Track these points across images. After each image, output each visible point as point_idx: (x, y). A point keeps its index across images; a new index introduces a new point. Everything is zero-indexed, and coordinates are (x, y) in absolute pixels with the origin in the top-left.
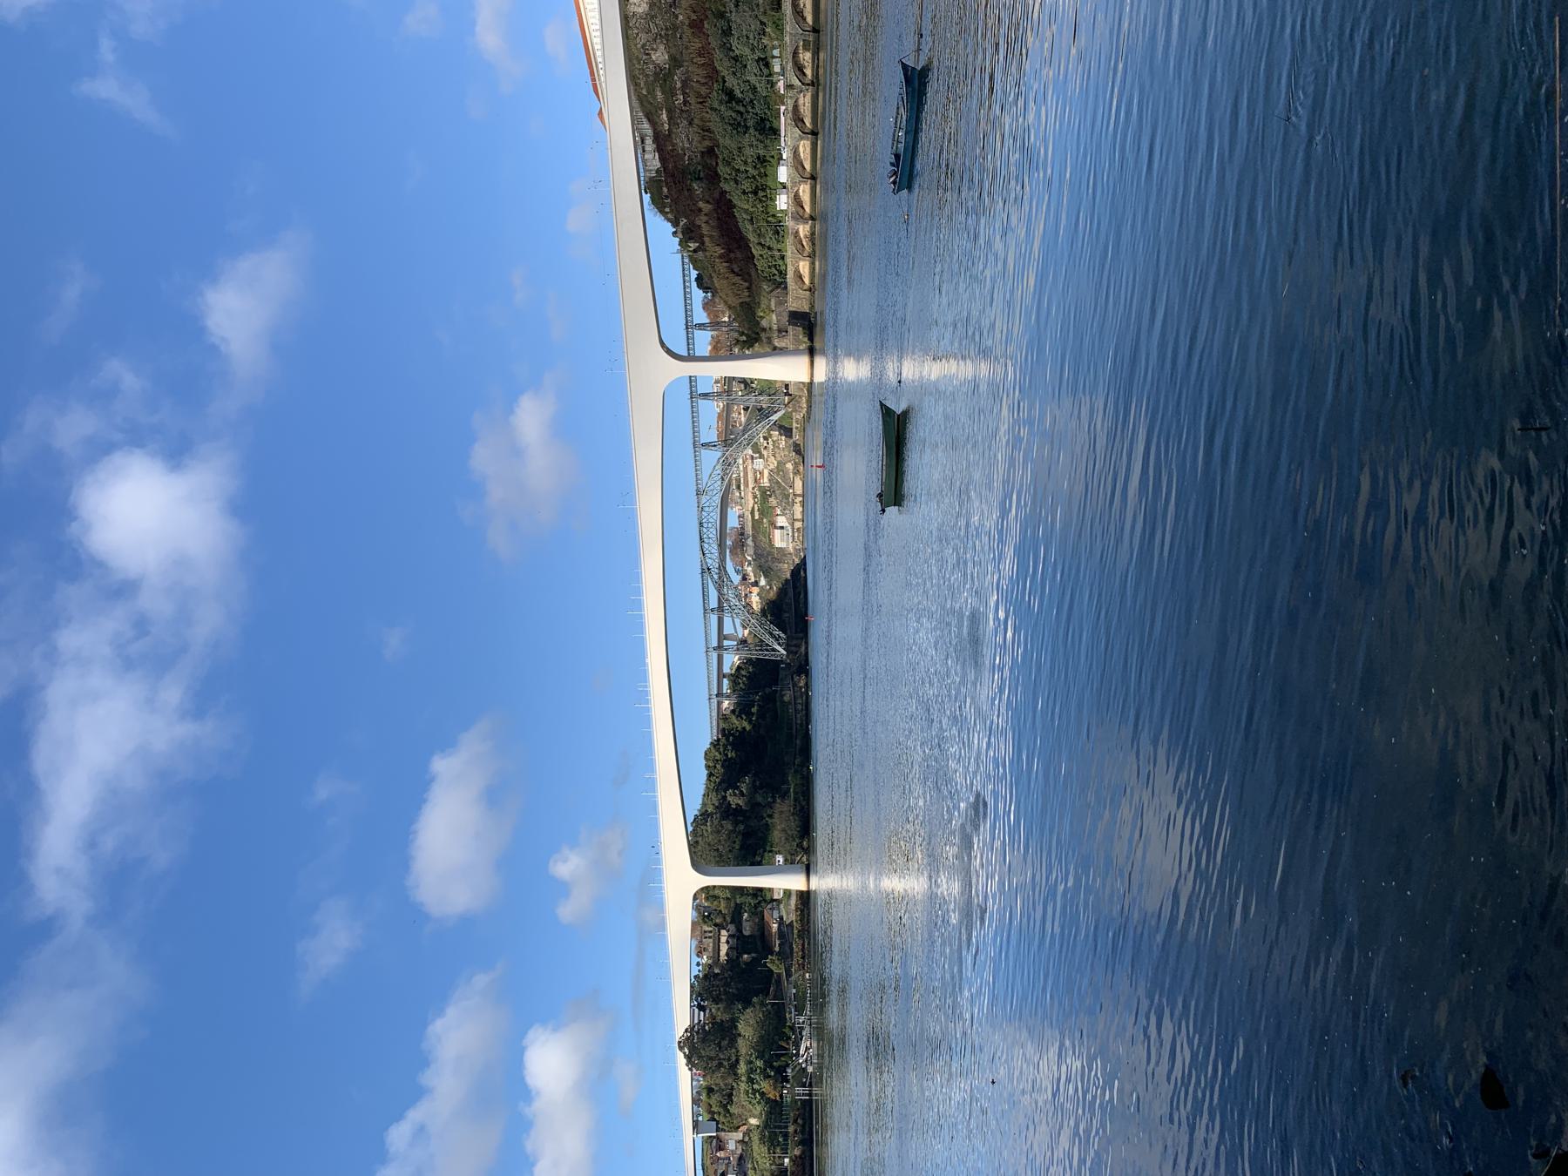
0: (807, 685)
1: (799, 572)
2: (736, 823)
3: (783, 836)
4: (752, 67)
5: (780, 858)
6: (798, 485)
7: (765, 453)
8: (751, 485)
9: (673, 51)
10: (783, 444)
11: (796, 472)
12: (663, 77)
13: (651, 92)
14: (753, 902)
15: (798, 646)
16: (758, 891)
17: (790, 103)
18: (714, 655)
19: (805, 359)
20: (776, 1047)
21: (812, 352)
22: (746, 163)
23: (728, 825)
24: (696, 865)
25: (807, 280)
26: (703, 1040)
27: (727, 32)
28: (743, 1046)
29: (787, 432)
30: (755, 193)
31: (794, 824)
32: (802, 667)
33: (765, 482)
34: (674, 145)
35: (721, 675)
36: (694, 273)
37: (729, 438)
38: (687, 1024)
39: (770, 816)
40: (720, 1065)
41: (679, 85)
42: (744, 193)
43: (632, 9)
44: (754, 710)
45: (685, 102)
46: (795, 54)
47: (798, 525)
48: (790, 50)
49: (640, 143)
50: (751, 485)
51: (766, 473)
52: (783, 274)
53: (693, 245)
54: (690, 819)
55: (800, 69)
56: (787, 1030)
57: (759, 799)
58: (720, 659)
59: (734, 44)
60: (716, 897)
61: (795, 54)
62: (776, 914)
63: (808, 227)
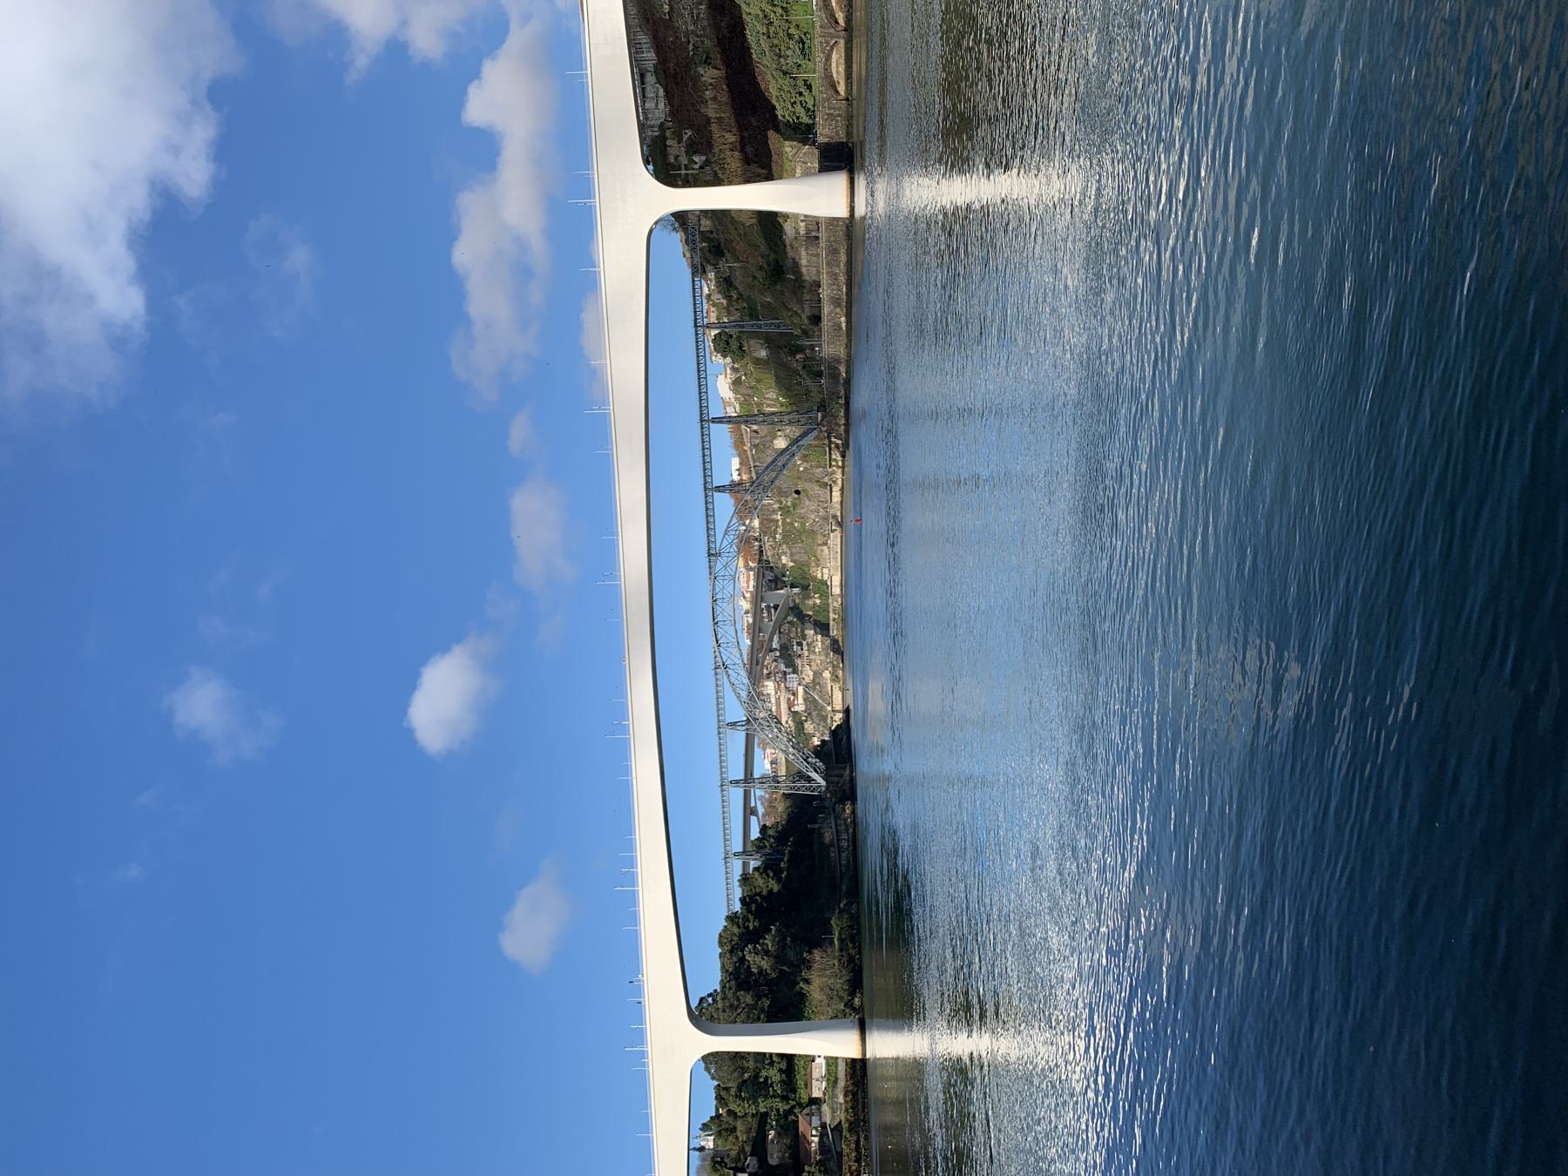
2: (758, 997)
6: (838, 696)
7: (798, 662)
10: (819, 647)
11: (835, 678)
14: (783, 1107)
16: (789, 1058)
29: (823, 628)
31: (840, 984)
33: (800, 707)
34: (676, 31)
39: (807, 981)
49: (639, 77)
51: (801, 689)
54: (694, 1004)
62: (816, 1121)
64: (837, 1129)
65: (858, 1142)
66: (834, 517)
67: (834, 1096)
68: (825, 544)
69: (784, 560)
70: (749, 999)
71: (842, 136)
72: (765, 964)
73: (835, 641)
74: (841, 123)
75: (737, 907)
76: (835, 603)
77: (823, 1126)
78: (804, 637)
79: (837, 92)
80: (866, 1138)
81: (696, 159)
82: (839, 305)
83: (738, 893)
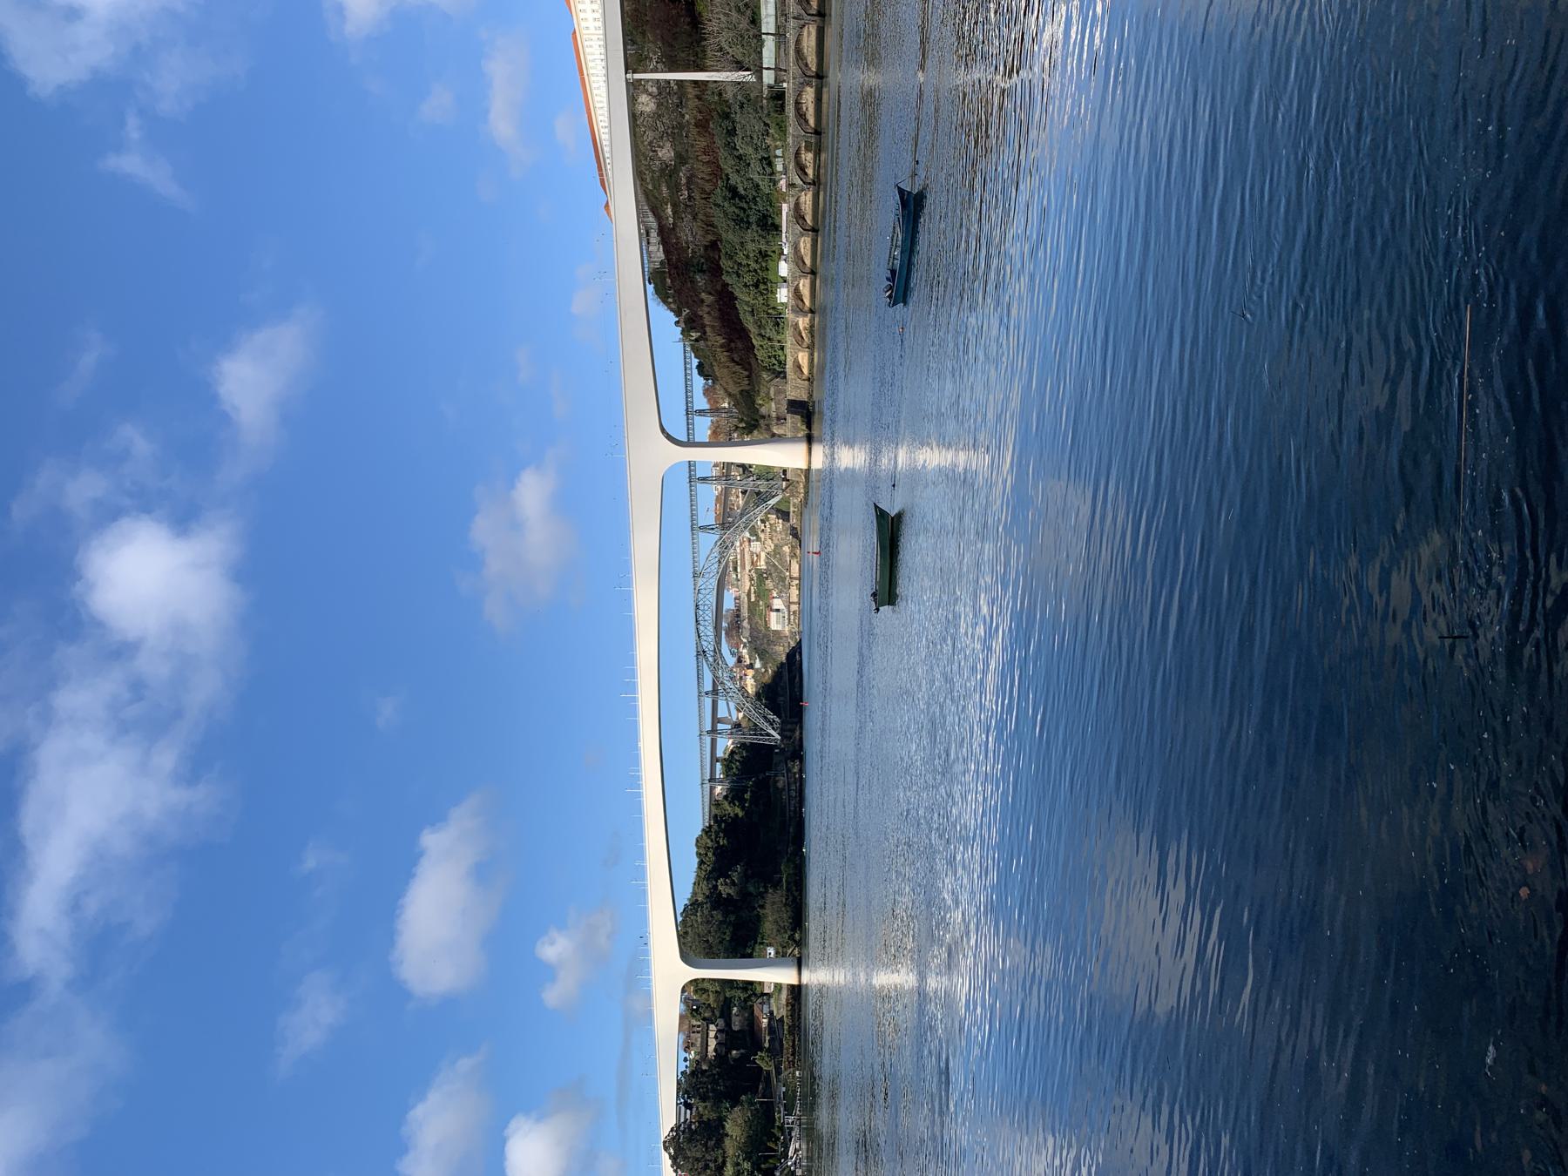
0: (801, 771)
1: (795, 655)
2: (726, 914)
3: (775, 927)
4: (755, 166)
5: (771, 951)
8: (748, 567)
9: (679, 148)
11: (793, 555)
12: (668, 173)
13: (657, 187)
14: (743, 996)
15: (793, 731)
16: (748, 985)
17: (792, 200)
18: (708, 739)
19: (803, 447)
20: (764, 1143)
21: (810, 440)
22: (747, 257)
23: (718, 915)
24: (685, 957)
25: (806, 371)
26: (690, 1140)
27: (732, 132)
28: (730, 1147)
29: (784, 515)
30: (756, 286)
31: (786, 915)
32: (795, 752)
33: (762, 565)
35: (714, 760)
36: (695, 362)
37: (726, 522)
38: (673, 1122)
39: (762, 907)
40: (706, 1167)
41: (684, 181)
42: (746, 285)
43: (640, 108)
44: (747, 796)
45: (690, 197)
46: (797, 154)
47: (794, 607)
48: (792, 151)
49: (645, 235)
50: (748, 567)
51: (763, 555)
52: (782, 364)
53: (695, 335)
54: (680, 909)
55: (801, 168)
56: (775, 1131)
57: (751, 889)
58: (714, 742)
59: (738, 142)
60: (705, 991)
61: (797, 154)
63: (807, 320)
70: (720, 917)
71: (805, 398)
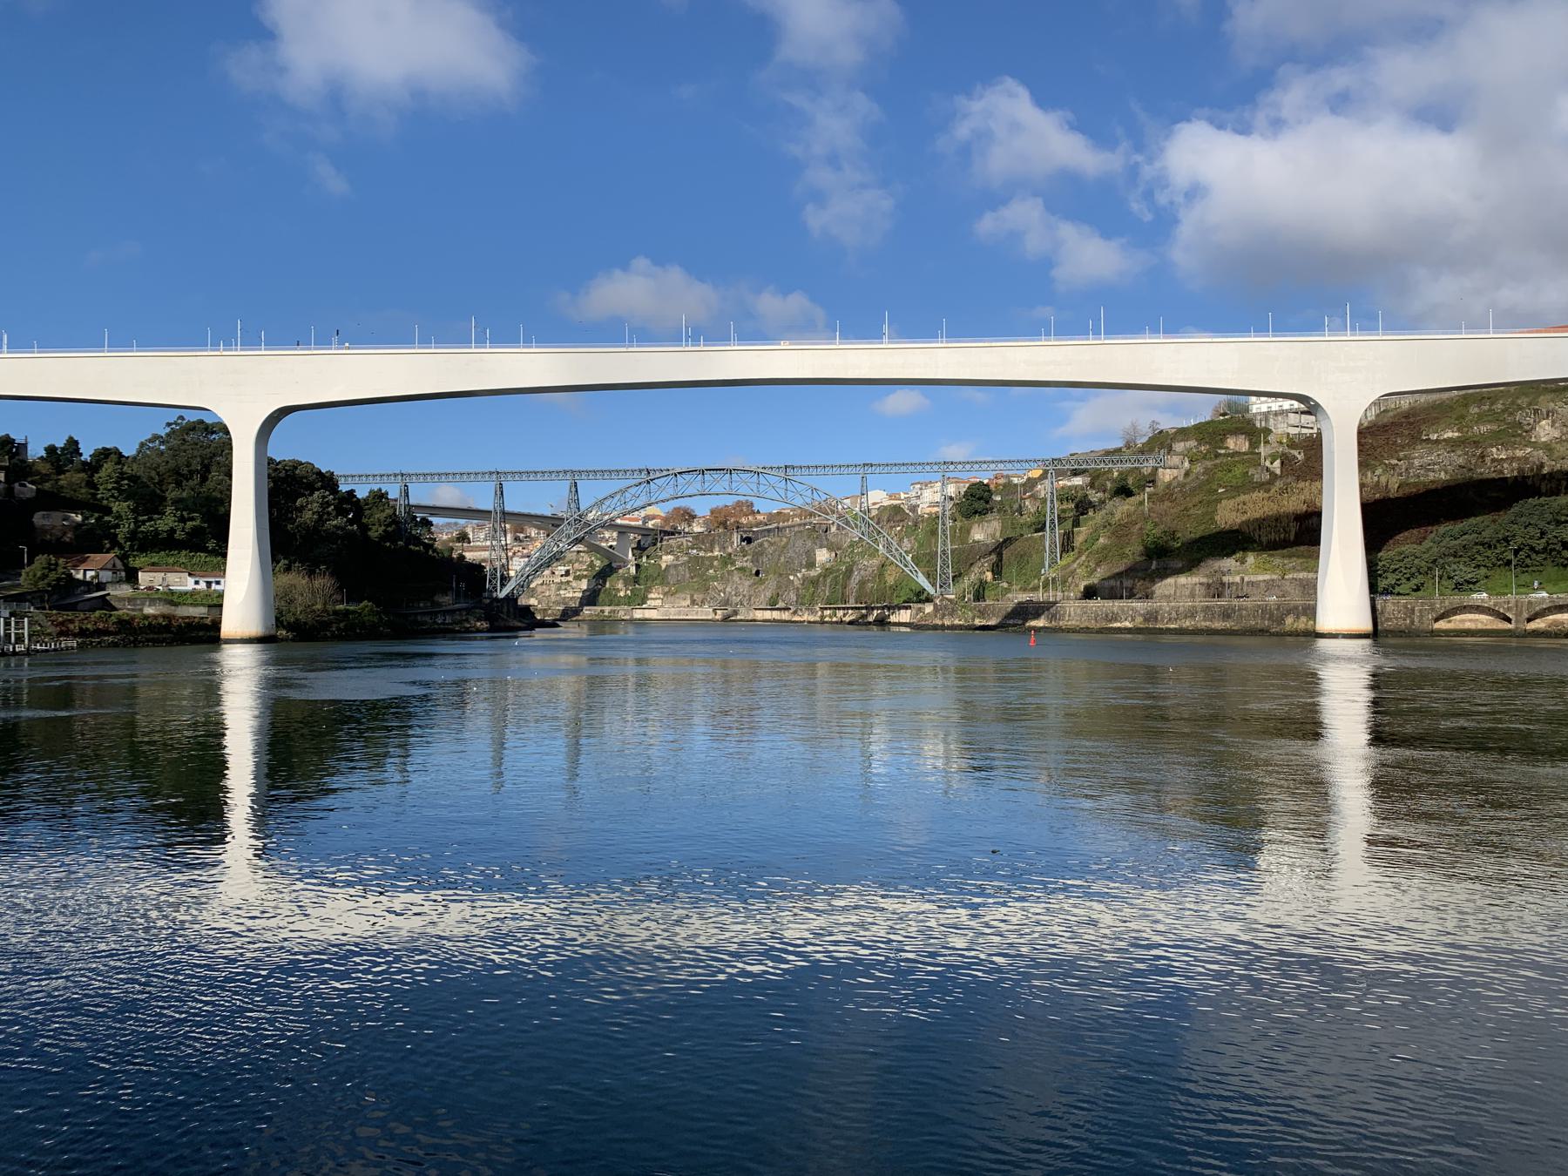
13: (1480, 419)
14: (122, 532)
29: (591, 598)
41: (1519, 453)
62: (106, 576)
64: (104, 603)
65: (106, 632)
66: (736, 613)
67: (153, 602)
68: (693, 602)
69: (667, 559)
72: (308, 516)
73: (576, 612)
74: (1403, 623)
75: (343, 488)
76: (622, 612)
77: (101, 586)
78: (578, 578)
79: (1437, 620)
80: (115, 645)
81: (1277, 463)
82: (1146, 620)
83: (362, 493)
